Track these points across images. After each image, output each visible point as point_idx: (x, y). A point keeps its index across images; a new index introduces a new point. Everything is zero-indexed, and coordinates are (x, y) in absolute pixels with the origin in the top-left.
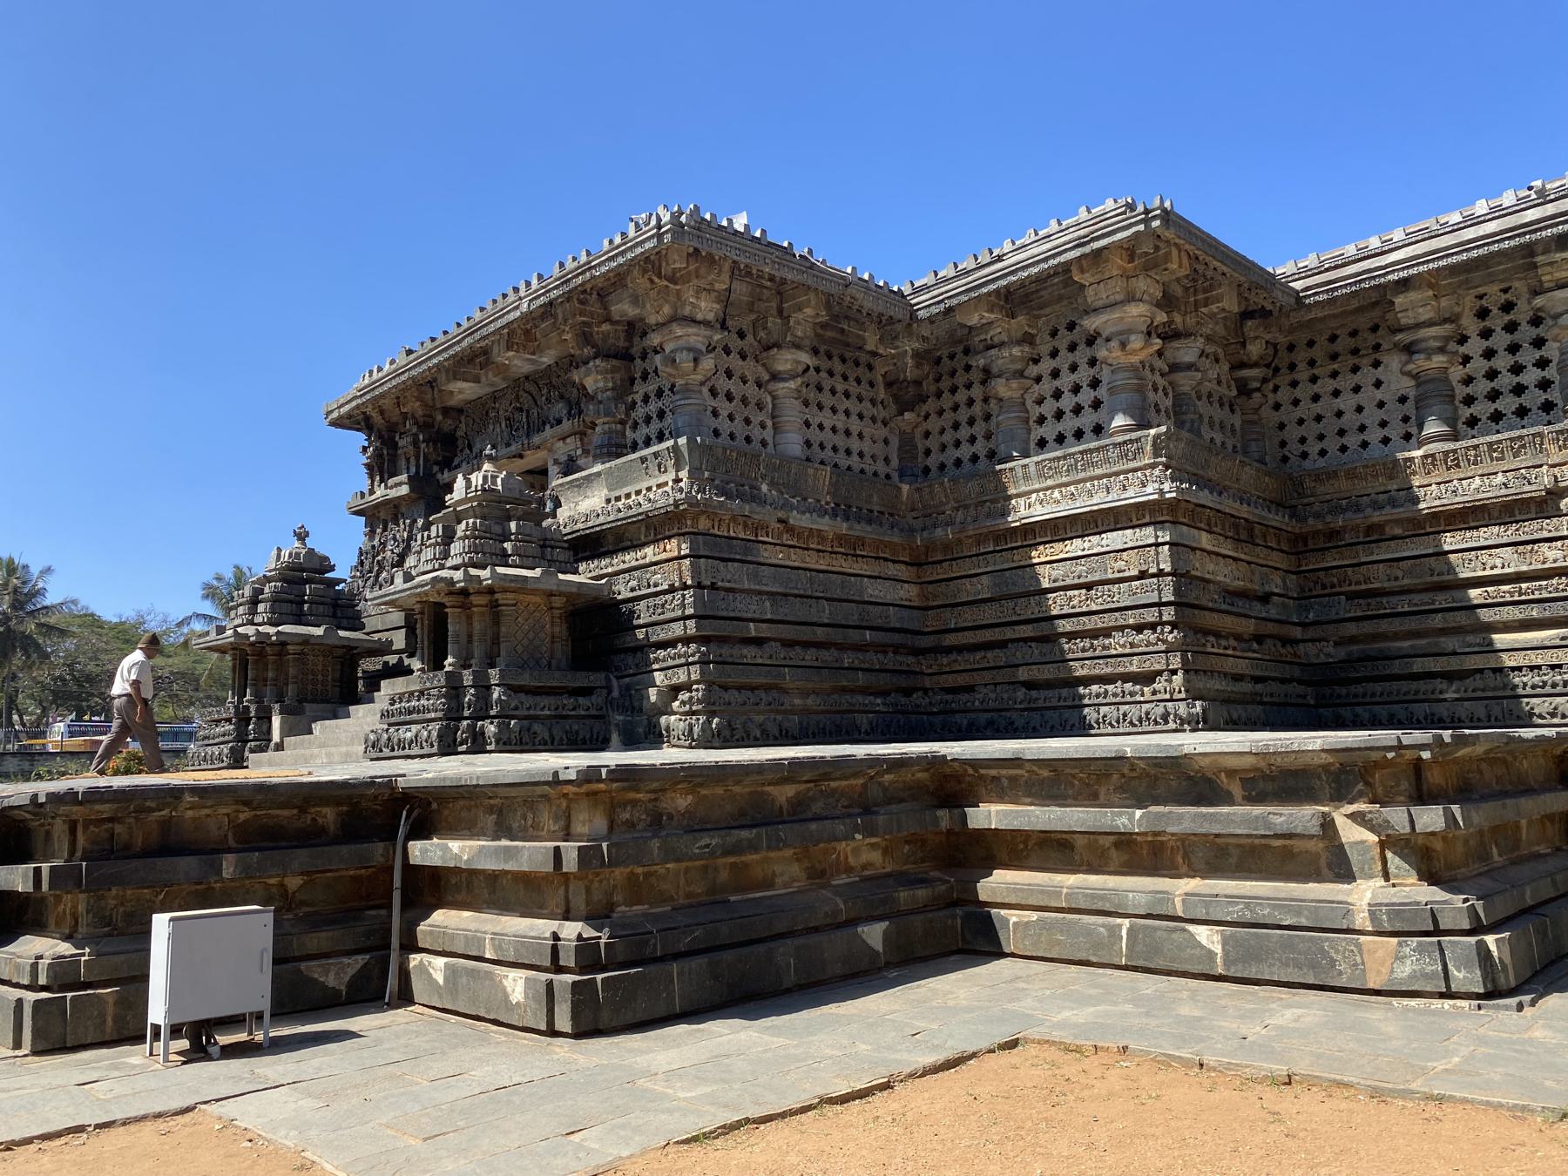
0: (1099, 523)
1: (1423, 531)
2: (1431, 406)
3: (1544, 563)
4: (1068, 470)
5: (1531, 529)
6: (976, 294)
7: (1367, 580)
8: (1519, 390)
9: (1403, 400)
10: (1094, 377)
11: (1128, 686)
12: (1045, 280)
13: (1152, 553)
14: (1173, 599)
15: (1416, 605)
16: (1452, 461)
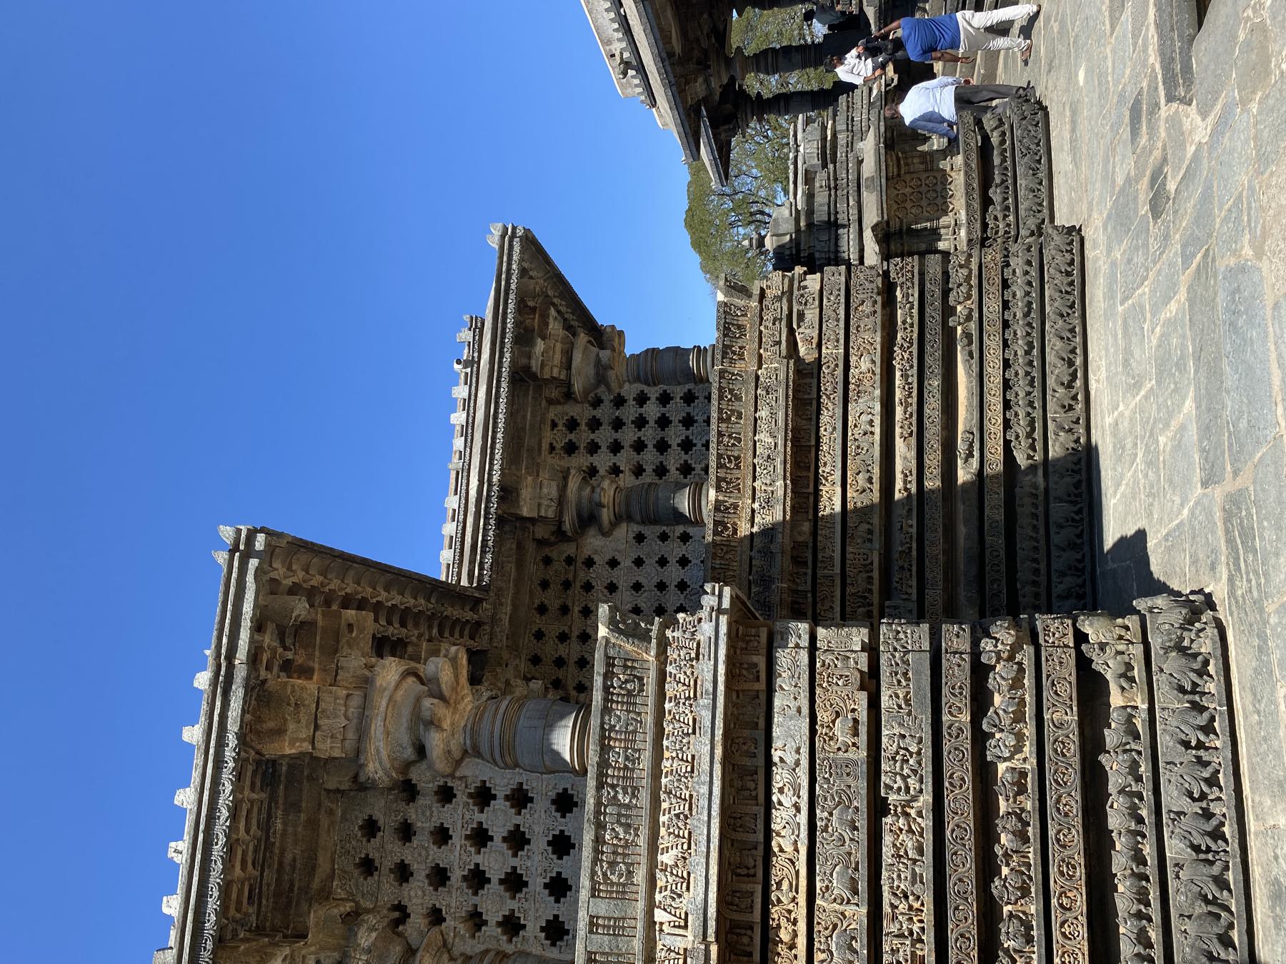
0: (747, 762)
1: (812, 498)
2: (657, 498)
3: (873, 373)
4: (627, 826)
5: (830, 381)
6: (210, 945)
7: (867, 568)
8: (663, 422)
9: (640, 538)
10: (470, 796)
11: (1112, 737)
12: (269, 846)
13: (829, 658)
14: (925, 627)
15: (910, 510)
16: (730, 461)
